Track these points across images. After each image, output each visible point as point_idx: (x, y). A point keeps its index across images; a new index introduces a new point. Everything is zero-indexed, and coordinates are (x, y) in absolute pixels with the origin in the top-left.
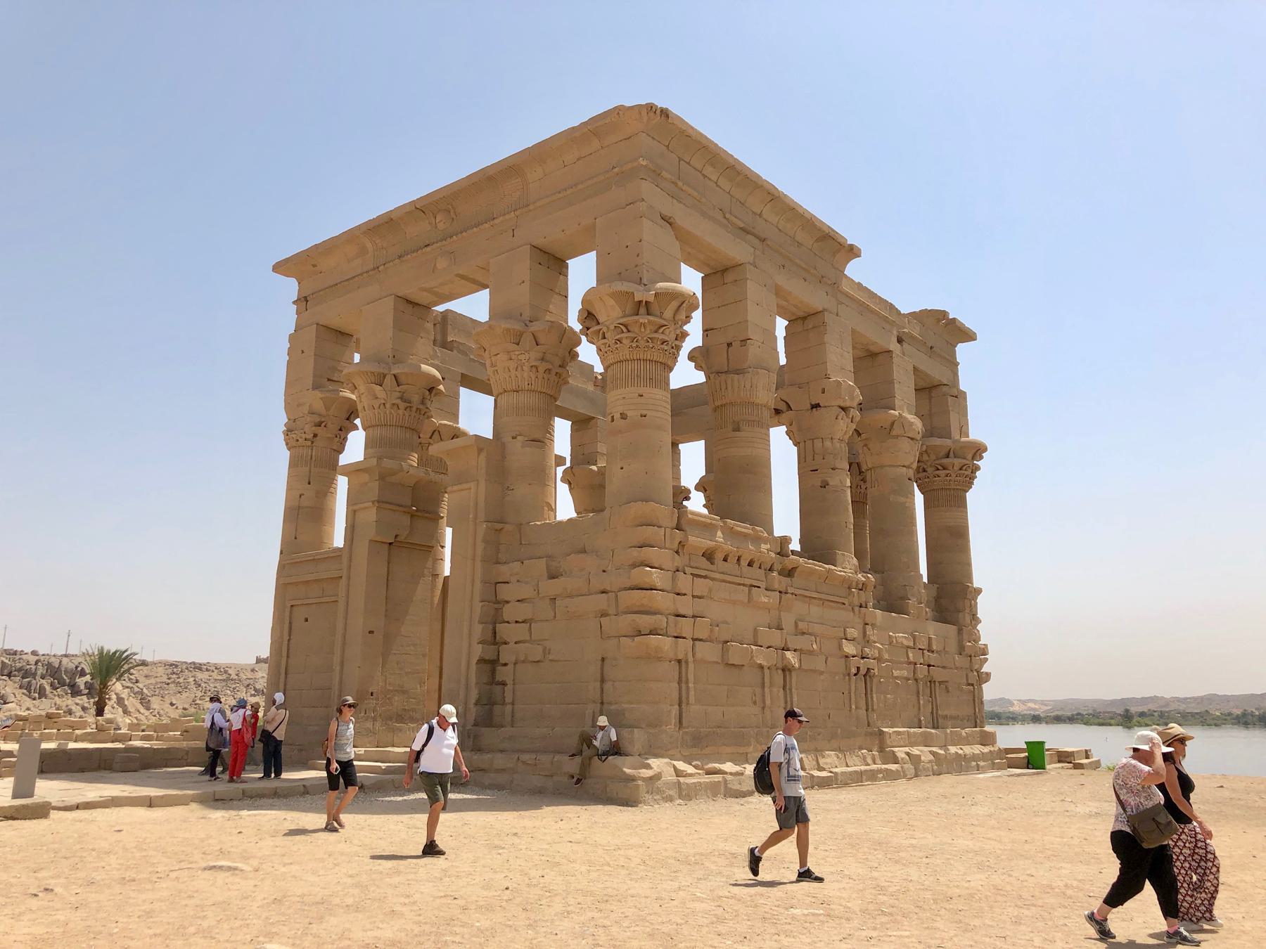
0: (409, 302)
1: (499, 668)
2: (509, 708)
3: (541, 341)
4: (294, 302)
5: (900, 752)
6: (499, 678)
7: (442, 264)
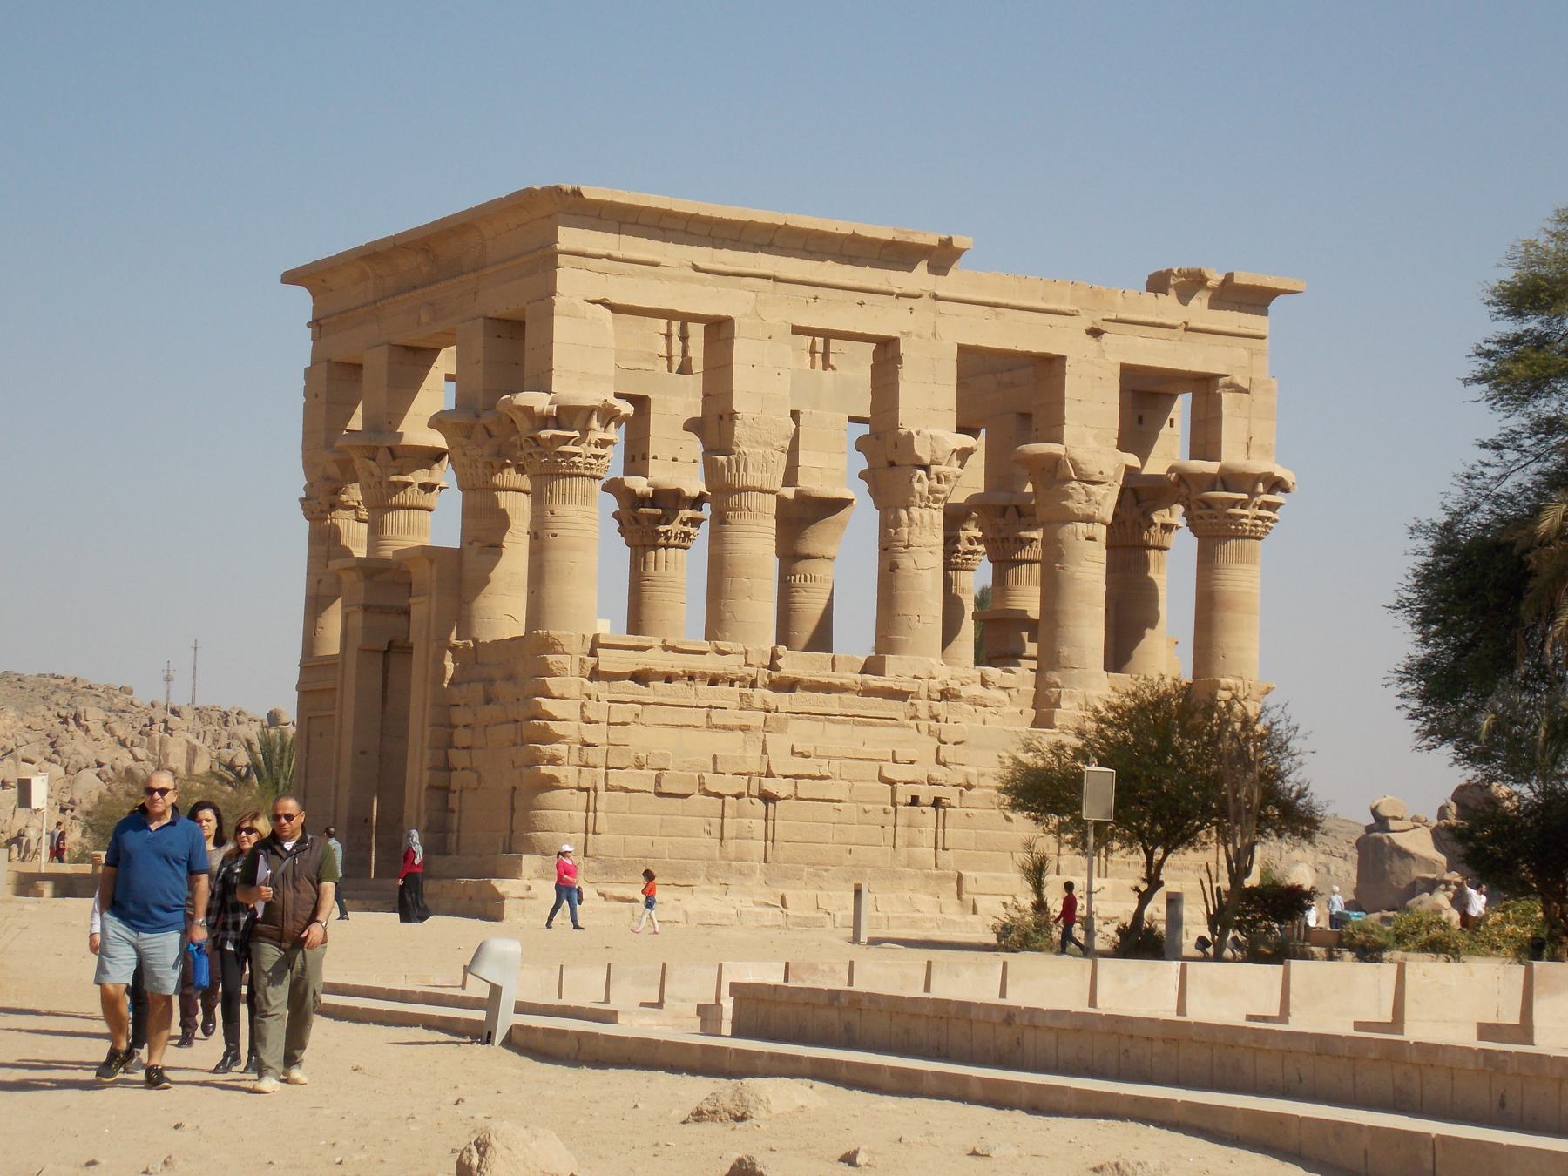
0: (408, 348)
1: (451, 795)
2: (454, 837)
3: (494, 430)
4: (309, 325)
5: (982, 903)
6: (451, 806)
7: (425, 318)
